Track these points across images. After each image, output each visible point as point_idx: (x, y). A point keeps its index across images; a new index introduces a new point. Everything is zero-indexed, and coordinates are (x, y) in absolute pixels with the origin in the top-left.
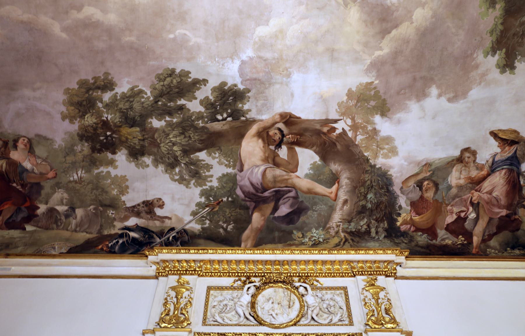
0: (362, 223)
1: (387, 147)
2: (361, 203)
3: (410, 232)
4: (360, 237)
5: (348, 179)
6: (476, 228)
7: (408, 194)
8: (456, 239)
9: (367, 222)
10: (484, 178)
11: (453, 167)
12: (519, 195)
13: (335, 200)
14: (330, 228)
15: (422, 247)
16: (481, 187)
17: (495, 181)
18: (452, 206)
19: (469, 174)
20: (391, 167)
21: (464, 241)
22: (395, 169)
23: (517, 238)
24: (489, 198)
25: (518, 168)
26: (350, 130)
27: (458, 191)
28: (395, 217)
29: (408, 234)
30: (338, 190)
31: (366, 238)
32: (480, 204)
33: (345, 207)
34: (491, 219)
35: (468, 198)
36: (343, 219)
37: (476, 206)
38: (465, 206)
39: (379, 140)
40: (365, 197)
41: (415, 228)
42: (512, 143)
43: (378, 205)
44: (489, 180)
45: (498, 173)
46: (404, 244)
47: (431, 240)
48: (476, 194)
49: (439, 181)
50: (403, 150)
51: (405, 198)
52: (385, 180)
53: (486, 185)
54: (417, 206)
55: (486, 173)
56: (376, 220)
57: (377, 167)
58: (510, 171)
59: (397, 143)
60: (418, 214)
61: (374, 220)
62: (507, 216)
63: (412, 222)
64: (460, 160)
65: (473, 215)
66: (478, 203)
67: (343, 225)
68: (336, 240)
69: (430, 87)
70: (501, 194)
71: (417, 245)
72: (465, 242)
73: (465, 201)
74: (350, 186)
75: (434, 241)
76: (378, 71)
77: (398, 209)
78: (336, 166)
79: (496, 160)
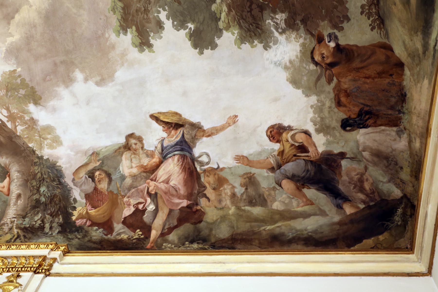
0: (36, 218)
1: (49, 136)
2: (35, 197)
3: (85, 227)
4: (33, 233)
5: (19, 172)
6: (156, 221)
7: (81, 185)
8: (132, 234)
9: (41, 217)
10: (158, 166)
11: (122, 155)
12: (198, 184)
13: (8, 195)
14: (4, 224)
15: (94, 243)
16: (156, 176)
17: (170, 168)
18: (128, 197)
19: (140, 162)
20: (58, 158)
21: (142, 235)
22: (64, 160)
23: (199, 231)
24: (166, 188)
25: (191, 154)
26: (8, 121)
27: (133, 181)
28: (71, 211)
29: (83, 229)
30: (9, 184)
31: (39, 234)
32: (158, 195)
33: (19, 201)
34: (171, 211)
35: (144, 189)
36: (18, 215)
37: (154, 197)
38: (143, 197)
39: (39, 130)
40: (38, 190)
41: (90, 223)
42: (177, 126)
43: (52, 199)
44: (163, 167)
45: (170, 160)
46: (77, 240)
47: (106, 235)
48: (152, 184)
49: (111, 171)
50: (66, 139)
51: (79, 191)
52: (55, 172)
53: (162, 173)
54: (92, 198)
55: (158, 160)
56: (51, 215)
57: (45, 158)
58: (183, 157)
59: (59, 132)
60: (94, 207)
61: (48, 214)
62: (188, 207)
63: (88, 216)
64: (127, 147)
65: (151, 207)
66: (156, 194)
67: (17, 221)
68: (8, 237)
69: (73, 72)
70: (179, 183)
71: (90, 241)
72: (142, 237)
73: (142, 191)
74: (21, 179)
75: (109, 236)
76: (17, 58)
77: (73, 202)
78: (4, 159)
79: (165, 145)
